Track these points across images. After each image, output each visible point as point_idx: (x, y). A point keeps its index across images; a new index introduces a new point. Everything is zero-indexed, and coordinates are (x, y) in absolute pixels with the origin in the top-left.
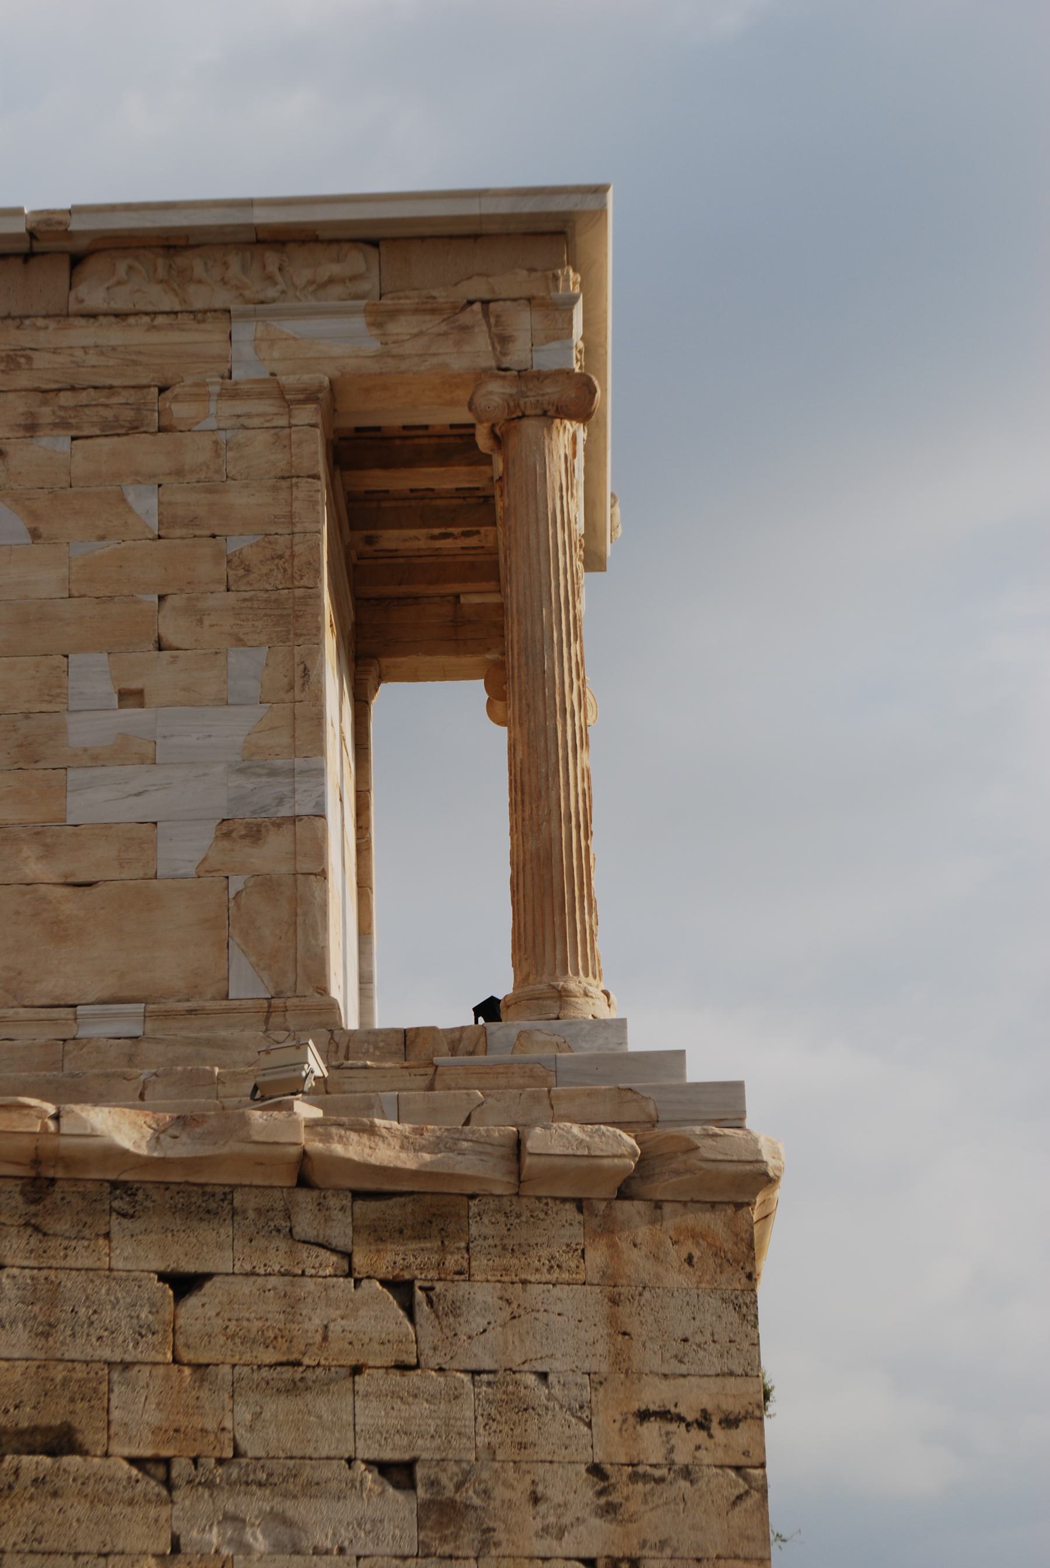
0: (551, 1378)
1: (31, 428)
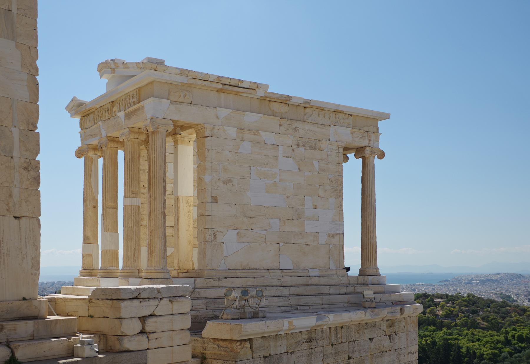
0: (402, 349)
1: (298, 145)
